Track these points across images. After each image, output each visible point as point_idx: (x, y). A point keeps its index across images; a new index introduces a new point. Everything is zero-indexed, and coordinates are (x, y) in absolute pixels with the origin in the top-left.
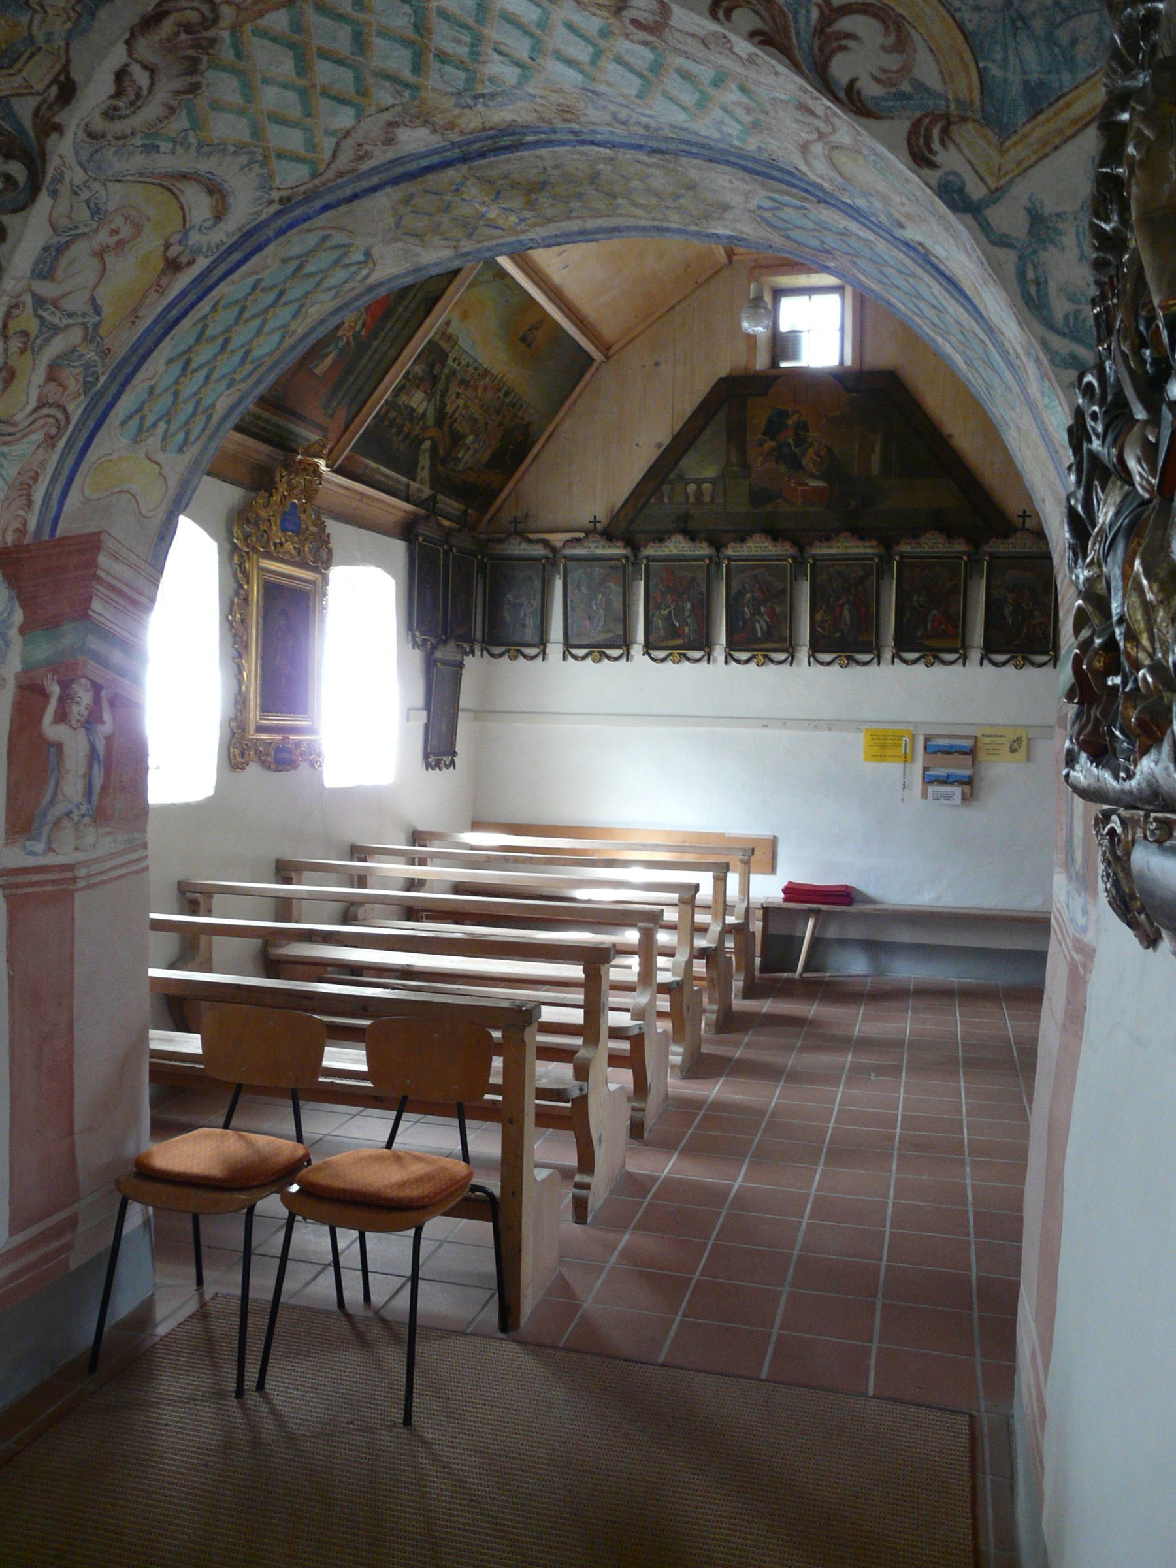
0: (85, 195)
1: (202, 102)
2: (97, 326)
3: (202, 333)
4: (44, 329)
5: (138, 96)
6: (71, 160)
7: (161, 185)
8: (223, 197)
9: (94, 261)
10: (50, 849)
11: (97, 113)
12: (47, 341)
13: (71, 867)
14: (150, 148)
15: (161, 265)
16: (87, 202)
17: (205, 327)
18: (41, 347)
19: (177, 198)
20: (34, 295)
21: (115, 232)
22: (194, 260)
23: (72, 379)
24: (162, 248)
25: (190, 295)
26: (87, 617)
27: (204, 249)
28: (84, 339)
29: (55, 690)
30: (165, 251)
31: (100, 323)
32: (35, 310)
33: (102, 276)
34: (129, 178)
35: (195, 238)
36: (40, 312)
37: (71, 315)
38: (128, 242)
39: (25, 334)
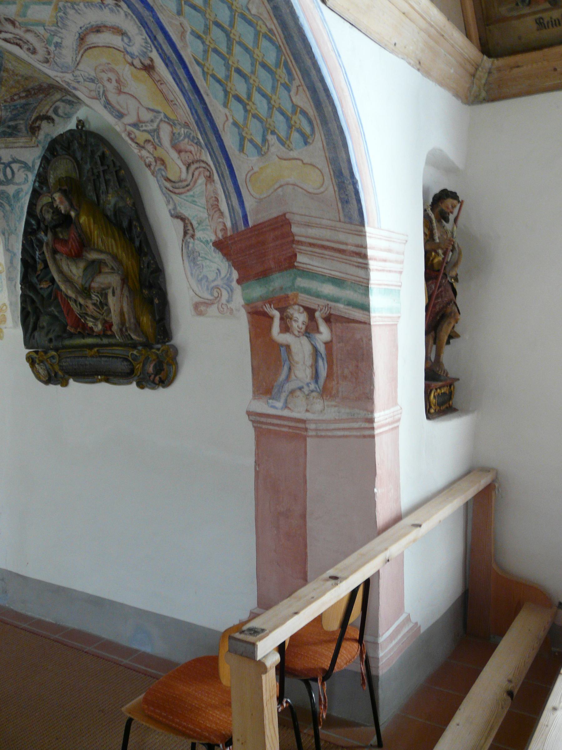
0: (81, 79)
2: (166, 116)
4: (152, 134)
6: (60, 74)
7: (86, 50)
8: (105, 26)
9: (123, 96)
10: (286, 406)
11: (33, 56)
12: (158, 137)
13: (304, 421)
14: (58, 45)
15: (144, 73)
16: (85, 80)
18: (160, 141)
19: (98, 47)
20: (129, 125)
21: (109, 80)
22: (150, 58)
24: (133, 67)
26: (294, 267)
27: (145, 50)
28: (171, 126)
29: (276, 314)
30: (135, 67)
31: (165, 115)
32: (138, 129)
33: (136, 98)
34: (78, 59)
35: (135, 49)
36: (141, 129)
37: (152, 121)
38: (119, 78)
39: (147, 141)
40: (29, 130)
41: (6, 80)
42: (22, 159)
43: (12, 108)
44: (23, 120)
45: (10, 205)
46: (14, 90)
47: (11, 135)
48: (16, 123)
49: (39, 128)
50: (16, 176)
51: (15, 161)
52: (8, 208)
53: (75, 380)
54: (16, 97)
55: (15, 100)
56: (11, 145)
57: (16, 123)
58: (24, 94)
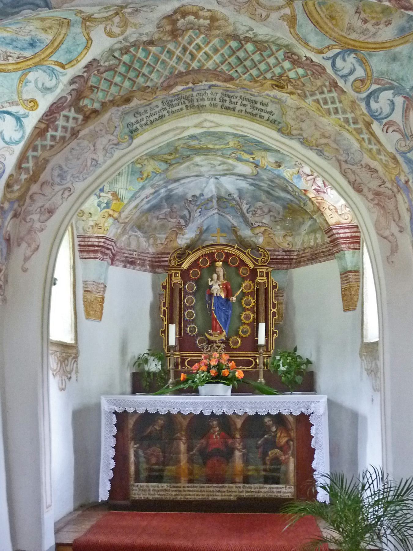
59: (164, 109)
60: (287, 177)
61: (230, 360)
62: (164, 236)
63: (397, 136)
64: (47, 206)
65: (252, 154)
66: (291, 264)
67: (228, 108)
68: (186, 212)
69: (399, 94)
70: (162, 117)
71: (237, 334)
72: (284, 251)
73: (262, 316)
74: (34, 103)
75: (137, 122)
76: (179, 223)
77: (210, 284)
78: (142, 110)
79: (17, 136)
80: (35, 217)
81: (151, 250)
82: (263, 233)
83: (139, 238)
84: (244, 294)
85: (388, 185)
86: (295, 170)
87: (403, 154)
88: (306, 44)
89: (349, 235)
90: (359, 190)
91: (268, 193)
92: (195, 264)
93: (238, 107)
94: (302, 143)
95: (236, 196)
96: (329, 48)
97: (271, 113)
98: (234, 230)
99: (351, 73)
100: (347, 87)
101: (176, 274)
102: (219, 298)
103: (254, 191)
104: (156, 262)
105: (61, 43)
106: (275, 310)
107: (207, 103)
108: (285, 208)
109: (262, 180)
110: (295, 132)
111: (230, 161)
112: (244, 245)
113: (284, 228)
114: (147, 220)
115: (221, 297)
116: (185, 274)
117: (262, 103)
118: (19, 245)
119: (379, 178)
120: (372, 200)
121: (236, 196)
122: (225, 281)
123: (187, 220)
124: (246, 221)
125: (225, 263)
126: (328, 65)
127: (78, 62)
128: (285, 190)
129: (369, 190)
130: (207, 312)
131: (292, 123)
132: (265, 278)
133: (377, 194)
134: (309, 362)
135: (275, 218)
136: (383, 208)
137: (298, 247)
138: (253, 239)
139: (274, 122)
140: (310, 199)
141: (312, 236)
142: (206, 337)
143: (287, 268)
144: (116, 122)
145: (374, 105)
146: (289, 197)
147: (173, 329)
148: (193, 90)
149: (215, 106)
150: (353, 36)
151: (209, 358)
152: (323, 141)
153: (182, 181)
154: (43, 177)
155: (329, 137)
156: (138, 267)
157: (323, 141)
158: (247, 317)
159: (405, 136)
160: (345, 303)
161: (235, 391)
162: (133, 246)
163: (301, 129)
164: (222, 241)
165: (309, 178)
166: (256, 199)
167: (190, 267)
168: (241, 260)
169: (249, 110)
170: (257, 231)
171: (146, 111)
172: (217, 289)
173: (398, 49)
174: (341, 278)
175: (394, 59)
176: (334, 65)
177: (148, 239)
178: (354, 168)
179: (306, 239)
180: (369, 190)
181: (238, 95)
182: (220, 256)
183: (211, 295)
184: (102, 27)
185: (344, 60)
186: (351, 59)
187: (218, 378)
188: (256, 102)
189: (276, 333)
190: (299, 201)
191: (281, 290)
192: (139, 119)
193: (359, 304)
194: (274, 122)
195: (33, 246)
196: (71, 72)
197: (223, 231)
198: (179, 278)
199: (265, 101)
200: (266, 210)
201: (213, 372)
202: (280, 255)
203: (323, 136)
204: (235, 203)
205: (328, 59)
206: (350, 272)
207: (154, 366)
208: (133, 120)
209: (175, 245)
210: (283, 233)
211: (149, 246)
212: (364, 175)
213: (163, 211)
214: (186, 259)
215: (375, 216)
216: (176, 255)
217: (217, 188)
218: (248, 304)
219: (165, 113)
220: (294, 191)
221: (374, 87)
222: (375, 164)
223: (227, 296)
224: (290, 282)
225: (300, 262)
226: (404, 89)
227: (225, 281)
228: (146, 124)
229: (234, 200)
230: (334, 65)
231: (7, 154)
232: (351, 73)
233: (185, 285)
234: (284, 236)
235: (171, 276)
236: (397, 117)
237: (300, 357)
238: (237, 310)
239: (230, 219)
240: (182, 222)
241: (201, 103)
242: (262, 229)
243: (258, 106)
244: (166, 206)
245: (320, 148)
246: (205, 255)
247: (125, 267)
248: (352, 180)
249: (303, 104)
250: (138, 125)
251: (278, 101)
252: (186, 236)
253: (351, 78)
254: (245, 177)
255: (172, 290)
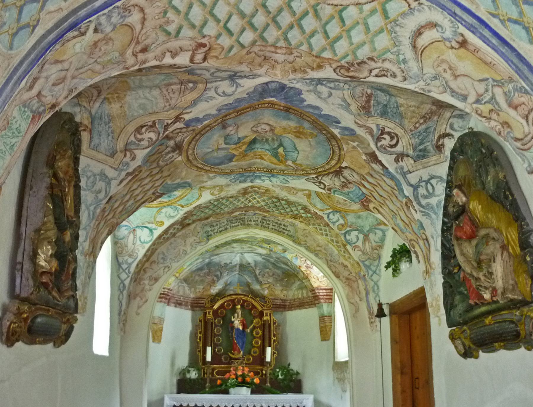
0: (429, 81)
1: (375, 54)
2: (494, 80)
3: (516, 22)
4: (492, 102)
5: (384, 70)
6: (416, 85)
7: (421, 54)
8: (422, 27)
9: (459, 79)
11: (396, 79)
12: (497, 103)
14: (404, 61)
15: (462, 50)
16: (432, 81)
17: (509, 20)
18: (499, 107)
19: (427, 47)
20: (474, 103)
21: (445, 71)
22: (460, 34)
23: (518, 98)
24: (454, 50)
25: (483, 33)
27: (454, 29)
28: (501, 87)
30: (455, 49)
31: (493, 79)
32: (481, 104)
33: (468, 76)
34: (420, 65)
35: (448, 34)
36: (483, 102)
37: (487, 91)
38: (450, 65)
39: (491, 111)
40: (435, 149)
41: (405, 114)
42: (438, 174)
43: (418, 134)
44: (429, 142)
45: (435, 214)
46: (414, 120)
47: (424, 157)
48: (424, 146)
49: (443, 145)
50: (436, 189)
51: (432, 177)
52: (433, 216)
53: (483, 352)
54: (417, 125)
55: (417, 128)
56: (426, 165)
57: (424, 146)
58: (422, 121)
59: (228, 224)
60: (289, 258)
61: (250, 372)
62: (202, 287)
63: (360, 253)
64: (154, 276)
65: (269, 244)
66: (285, 308)
67: (265, 227)
68: (219, 273)
69: (361, 233)
70: (226, 229)
71: (250, 354)
72: (281, 299)
73: (267, 342)
74: (162, 223)
75: (212, 231)
76: (213, 279)
77: (233, 320)
78: (214, 224)
79: (148, 239)
80: (146, 282)
81: (192, 296)
82: (268, 288)
83: (184, 287)
84: (254, 327)
85: (354, 274)
86: (294, 255)
87: (363, 262)
88: (315, 206)
89: (326, 294)
90: (338, 277)
91: (274, 264)
92: (222, 306)
93: (271, 227)
94: (306, 249)
95: (253, 265)
96: (326, 209)
97: (289, 231)
98: (248, 285)
99: (337, 221)
100: (335, 228)
101: (209, 312)
102: (238, 329)
103: (265, 262)
104: (194, 303)
105: (185, 196)
106: (275, 338)
107: (253, 223)
108: (283, 273)
109: (272, 257)
110: (302, 243)
111: (255, 247)
112: (255, 295)
113: (282, 285)
114: (192, 276)
115: (239, 329)
116: (215, 313)
117: (284, 225)
118: (135, 298)
119: (349, 270)
120: (345, 282)
121: (253, 265)
122: (242, 319)
123: (219, 278)
124: (257, 280)
125: (242, 306)
126: (325, 217)
127: (191, 205)
128: (286, 264)
129: (343, 277)
130: (229, 338)
131: (301, 237)
132: (269, 317)
133: (347, 279)
134: (298, 373)
135: (277, 278)
136: (351, 287)
137: (291, 297)
138: (261, 291)
139: (291, 236)
140: (302, 272)
141: (300, 292)
142: (229, 355)
143: (283, 311)
144: (199, 229)
145: (348, 237)
146: (288, 268)
147: (209, 350)
148: (245, 215)
149: (258, 225)
150: (339, 206)
151: (236, 370)
152: (318, 248)
153: (220, 255)
154: (152, 259)
155: (321, 247)
156: (183, 307)
157: (318, 248)
158: (257, 343)
159: (364, 253)
160: (323, 336)
161: (252, 393)
162: (181, 293)
163: (306, 241)
164: (239, 292)
165: (302, 259)
166: (266, 267)
167: (219, 308)
168: (253, 305)
169: (277, 228)
170: (264, 286)
171: (217, 225)
172: (237, 324)
173: (361, 213)
174: (320, 320)
175: (359, 217)
176: (328, 217)
177: (190, 288)
178: (335, 264)
179: (296, 293)
180: (343, 277)
181: (271, 220)
182: (239, 301)
183: (233, 327)
184: (209, 191)
185: (334, 215)
186: (337, 215)
187: (243, 383)
188: (281, 224)
189: (275, 353)
190: (294, 271)
191: (279, 325)
192: (213, 229)
193: (332, 337)
194: (291, 236)
195: (144, 300)
196: (186, 209)
197: (241, 285)
198: (211, 315)
199: (286, 224)
200: (271, 274)
201: (240, 379)
202: (278, 302)
203: (318, 246)
204: (251, 269)
205: (326, 214)
206: (326, 316)
207: (193, 375)
208: (209, 229)
209: (209, 293)
210: (281, 288)
211: (191, 292)
212: (341, 269)
213: (204, 271)
214: (216, 303)
215: (347, 291)
216: (209, 300)
217: (240, 259)
218: (257, 334)
219: (228, 227)
220: (292, 265)
221: (349, 229)
222: (346, 263)
223: (243, 328)
224: (284, 321)
225: (292, 307)
226: (363, 231)
227: (242, 319)
228: (217, 232)
229: (252, 267)
230: (328, 217)
231: (141, 249)
232: (337, 221)
233: (215, 320)
234: (282, 291)
235: (205, 314)
236: (360, 243)
237: (292, 370)
238: (250, 337)
239: (247, 278)
240: (215, 279)
241: (250, 223)
242: (268, 285)
243: (282, 226)
244: (206, 268)
245: (316, 252)
246: (229, 301)
247: (176, 307)
248: (334, 271)
249: (307, 228)
250: (212, 233)
251: (294, 225)
252: (217, 288)
253: (337, 224)
254: (261, 255)
255: (206, 323)
